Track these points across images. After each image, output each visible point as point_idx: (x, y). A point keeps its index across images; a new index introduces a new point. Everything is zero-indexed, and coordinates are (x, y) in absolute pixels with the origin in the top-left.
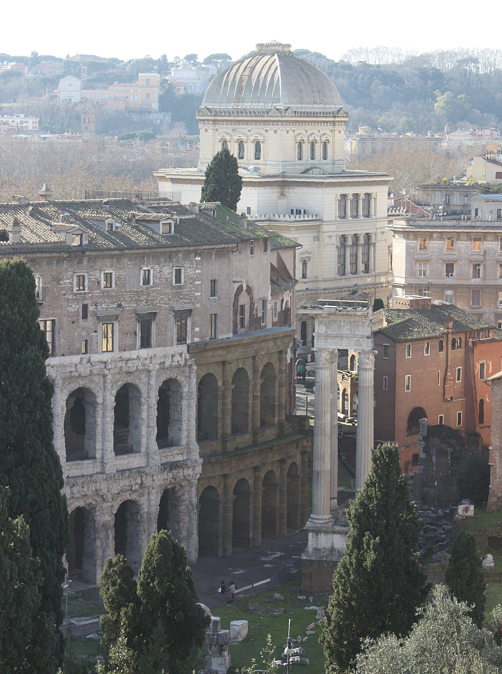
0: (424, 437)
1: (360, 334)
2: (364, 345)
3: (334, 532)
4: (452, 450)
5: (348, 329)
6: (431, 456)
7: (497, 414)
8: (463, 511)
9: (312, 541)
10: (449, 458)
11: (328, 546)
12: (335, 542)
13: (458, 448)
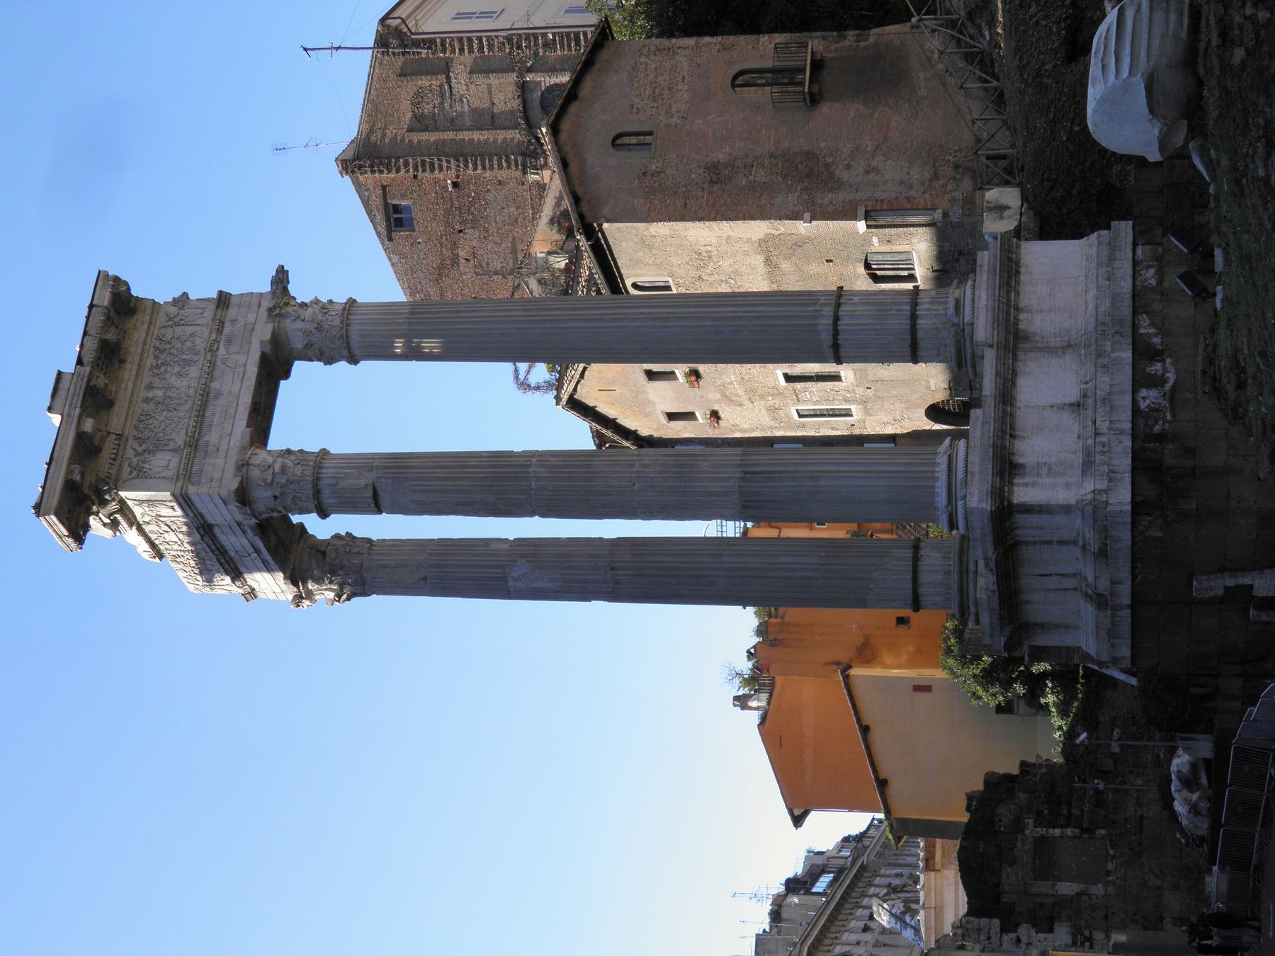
0: (1004, 929)
1: (207, 332)
2: (251, 318)
3: (1006, 396)
5: (179, 375)
6: (1062, 902)
8: (1001, 217)
9: (1053, 486)
10: (1057, 832)
12: (1052, 400)
13: (1022, 797)
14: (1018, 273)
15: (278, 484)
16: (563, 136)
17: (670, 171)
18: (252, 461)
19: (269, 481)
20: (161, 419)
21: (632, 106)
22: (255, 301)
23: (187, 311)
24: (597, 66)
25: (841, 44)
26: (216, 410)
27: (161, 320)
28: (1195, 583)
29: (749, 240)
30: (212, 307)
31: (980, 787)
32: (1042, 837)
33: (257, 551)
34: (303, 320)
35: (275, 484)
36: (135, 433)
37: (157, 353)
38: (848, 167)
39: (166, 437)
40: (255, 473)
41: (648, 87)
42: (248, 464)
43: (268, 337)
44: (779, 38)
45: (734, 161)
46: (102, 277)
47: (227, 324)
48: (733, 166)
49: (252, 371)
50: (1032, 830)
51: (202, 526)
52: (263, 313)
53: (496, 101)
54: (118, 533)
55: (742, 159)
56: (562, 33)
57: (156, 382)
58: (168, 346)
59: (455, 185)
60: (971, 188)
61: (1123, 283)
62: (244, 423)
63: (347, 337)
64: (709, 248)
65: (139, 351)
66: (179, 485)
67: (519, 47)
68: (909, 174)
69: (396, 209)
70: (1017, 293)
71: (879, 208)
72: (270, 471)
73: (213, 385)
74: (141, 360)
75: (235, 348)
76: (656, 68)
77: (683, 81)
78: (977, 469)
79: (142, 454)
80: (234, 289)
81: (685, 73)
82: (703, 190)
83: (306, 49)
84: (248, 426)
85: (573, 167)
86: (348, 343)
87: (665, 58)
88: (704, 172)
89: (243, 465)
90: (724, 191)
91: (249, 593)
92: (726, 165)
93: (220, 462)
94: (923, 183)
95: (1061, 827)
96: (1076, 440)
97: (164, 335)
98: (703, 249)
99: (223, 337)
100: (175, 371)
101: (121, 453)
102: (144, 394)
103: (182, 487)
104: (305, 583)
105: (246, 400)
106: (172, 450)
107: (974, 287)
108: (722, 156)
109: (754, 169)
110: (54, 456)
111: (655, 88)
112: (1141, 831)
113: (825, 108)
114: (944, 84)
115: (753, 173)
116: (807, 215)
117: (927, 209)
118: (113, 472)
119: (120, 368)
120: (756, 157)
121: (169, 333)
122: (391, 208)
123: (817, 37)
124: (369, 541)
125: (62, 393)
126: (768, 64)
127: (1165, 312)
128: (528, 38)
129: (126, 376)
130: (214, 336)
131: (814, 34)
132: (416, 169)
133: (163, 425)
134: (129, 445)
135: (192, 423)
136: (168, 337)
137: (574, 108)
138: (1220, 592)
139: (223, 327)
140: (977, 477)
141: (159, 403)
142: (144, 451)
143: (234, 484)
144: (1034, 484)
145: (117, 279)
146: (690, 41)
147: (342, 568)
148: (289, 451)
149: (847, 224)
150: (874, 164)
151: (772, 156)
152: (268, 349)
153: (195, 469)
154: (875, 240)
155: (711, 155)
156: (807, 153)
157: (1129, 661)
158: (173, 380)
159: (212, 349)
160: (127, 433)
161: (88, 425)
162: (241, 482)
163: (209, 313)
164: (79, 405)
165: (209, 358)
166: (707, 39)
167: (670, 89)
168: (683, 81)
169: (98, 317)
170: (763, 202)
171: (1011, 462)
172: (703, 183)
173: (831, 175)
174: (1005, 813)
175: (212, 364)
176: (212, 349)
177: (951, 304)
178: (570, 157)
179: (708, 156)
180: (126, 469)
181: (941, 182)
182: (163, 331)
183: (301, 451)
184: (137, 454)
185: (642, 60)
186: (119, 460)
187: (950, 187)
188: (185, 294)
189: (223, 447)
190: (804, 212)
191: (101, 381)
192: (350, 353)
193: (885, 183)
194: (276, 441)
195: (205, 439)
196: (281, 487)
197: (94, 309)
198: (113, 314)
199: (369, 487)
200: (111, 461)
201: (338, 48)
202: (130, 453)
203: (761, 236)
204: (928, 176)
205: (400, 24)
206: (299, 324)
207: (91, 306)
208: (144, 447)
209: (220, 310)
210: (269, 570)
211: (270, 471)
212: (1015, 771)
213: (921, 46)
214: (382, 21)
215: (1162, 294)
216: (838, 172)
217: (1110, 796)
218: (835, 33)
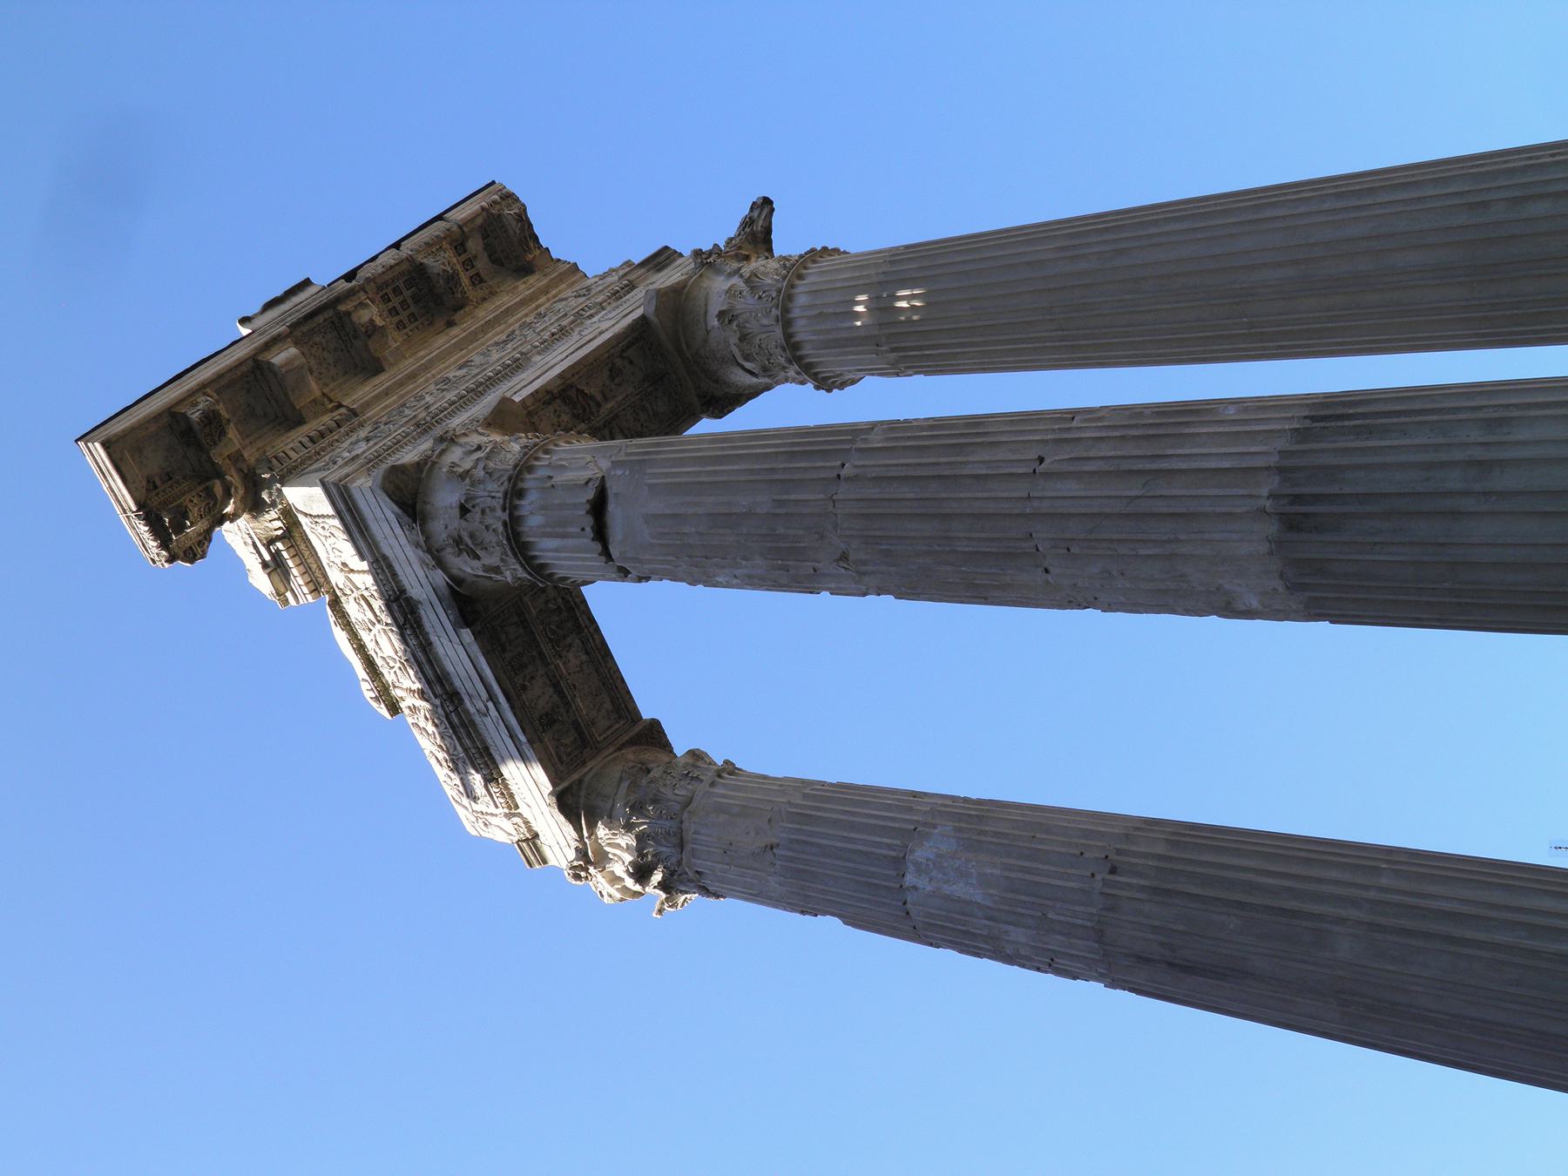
33: (492, 697)
51: (397, 599)
86: (786, 310)
91: (527, 840)
103: (347, 475)
104: (592, 827)
145: (509, 197)
147: (655, 801)
192: (788, 336)
199: (591, 484)
200: (305, 440)
207: (439, 217)
210: (524, 759)
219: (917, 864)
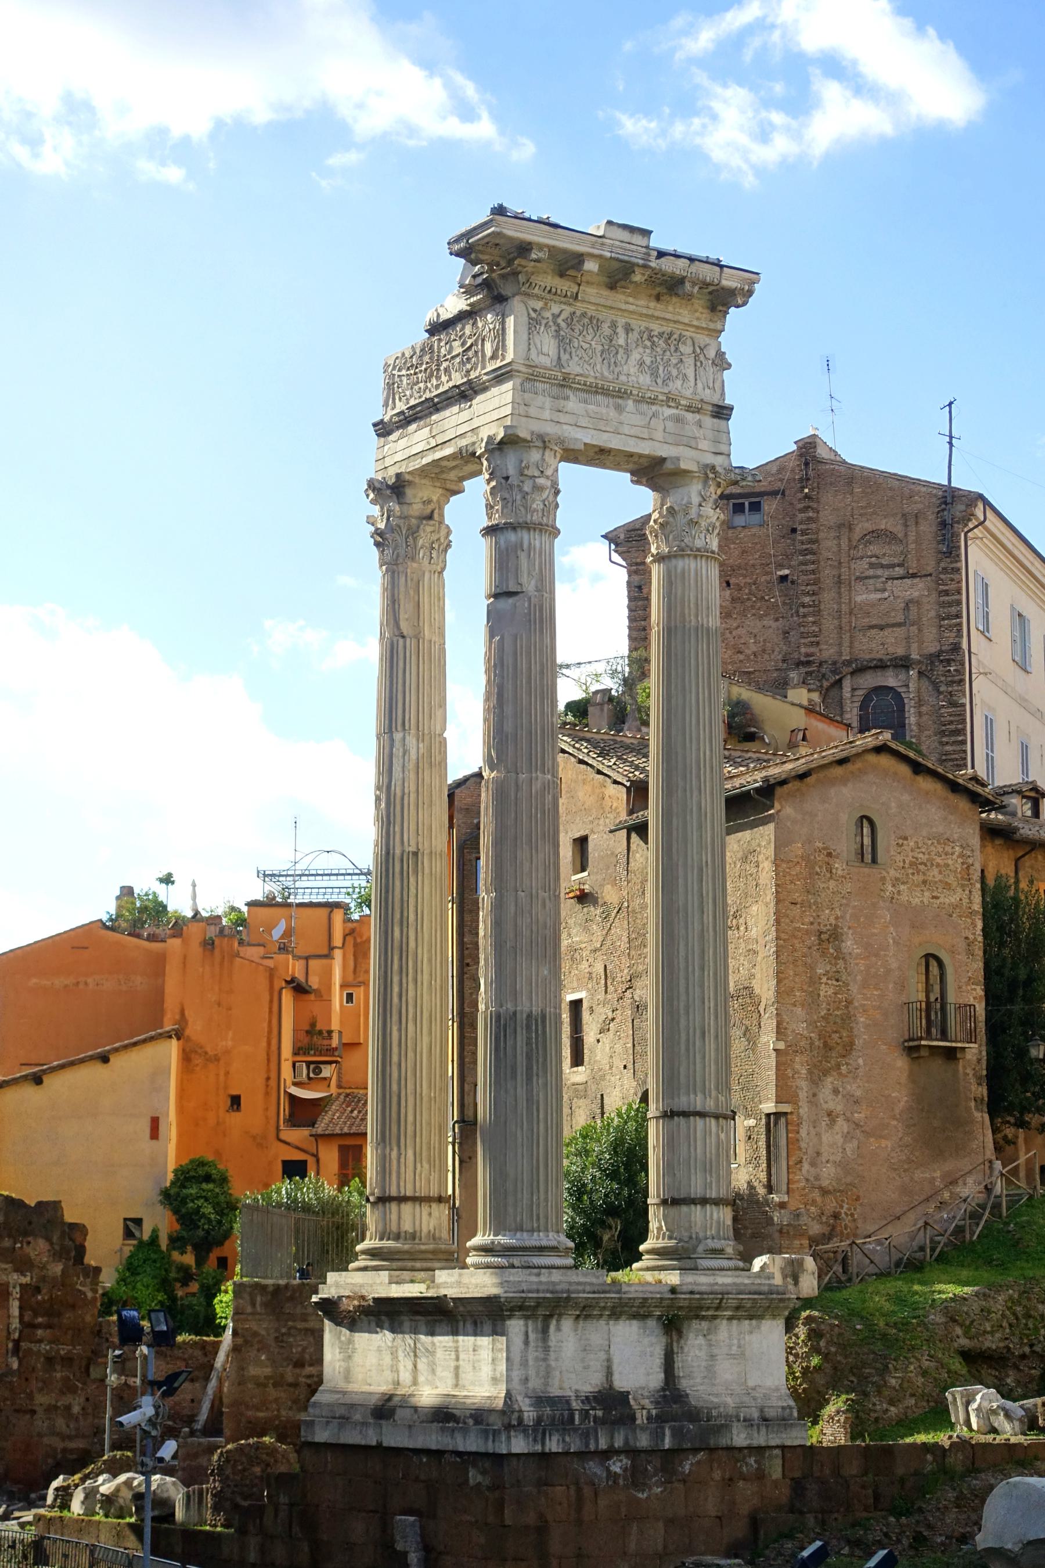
1: (688, 393)
4: (26, 1280)
5: (641, 363)
7: (797, 910)
10: (15, 1311)
11: (590, 1382)
12: (616, 1360)
13: (57, 1269)
14: (751, 1318)
15: (522, 482)
16: (872, 758)
17: (832, 884)
18: (547, 453)
19: (526, 472)
20: (593, 343)
21: (906, 839)
22: (723, 448)
23: (711, 370)
24: (951, 796)
25: (973, 1081)
26: (603, 406)
27: (702, 339)
28: (412, 1519)
29: (752, 976)
30: (715, 400)
31: (69, 1217)
32: (9, 1294)
34: (700, 505)
35: (521, 478)
36: (578, 313)
37: (665, 335)
38: (836, 1091)
39: (573, 350)
40: (535, 456)
41: (927, 856)
42: (545, 448)
43: (683, 466)
44: (980, 1009)
45: (843, 958)
46: (752, 277)
47: (697, 416)
48: (836, 958)
49: (645, 448)
50: (17, 1280)
51: (472, 388)
52: (710, 459)
53: (886, 632)
54: (462, 290)
55: (846, 968)
56: (964, 715)
57: (634, 336)
58: (673, 348)
59: (783, 579)
60: (811, 1233)
61: (743, 1436)
62: (588, 441)
63: (683, 556)
64: (742, 928)
65: (669, 316)
66: (523, 369)
67: (949, 662)
68: (827, 1162)
69: (756, 507)
70: (730, 1318)
71: (790, 1128)
72: (537, 473)
73: (630, 402)
74: (658, 318)
75: (670, 425)
76: (948, 865)
77: (934, 897)
78: (543, 1279)
79: (555, 323)
80: (734, 423)
81: (941, 900)
82: (812, 923)
83: (950, 404)
84: (585, 444)
85: (838, 771)
86: (675, 556)
87: (959, 876)
88: (831, 925)
89: (544, 442)
90: (810, 948)
92: (838, 949)
93: (547, 414)
94: (817, 1178)
95: (21, 1316)
96: (573, 1388)
97: (684, 343)
98: (742, 921)
99: (683, 413)
100: (645, 358)
101: (556, 298)
102: (621, 321)
103: (519, 372)
105: (614, 443)
106: (559, 358)
107: (737, 1269)
108: (849, 945)
109: (835, 983)
110: (560, 230)
111: (926, 865)
112: (17, 1411)
113: (901, 1063)
114: (927, 1200)
115: (829, 982)
116: (781, 1045)
117: (788, 1184)
118: (536, 291)
119: (650, 296)
120: (848, 985)
121: (686, 349)
122: (757, 500)
123: (980, 1052)
124: (443, 569)
125: (625, 236)
126: (951, 998)
127: (712, 1483)
128: (960, 672)
129: (642, 302)
130: (683, 402)
131: (984, 1048)
132: (804, 533)
133: (586, 346)
134: (563, 307)
135: (591, 380)
136: (682, 348)
137: (904, 770)
138: (399, 1547)
139: (693, 412)
140: (534, 1279)
141: (611, 341)
142: (558, 325)
143: (523, 434)
144: (526, 1342)
145: (750, 293)
146: (977, 906)
148: (557, 492)
149: (771, 1092)
150: (840, 1121)
151: (849, 1002)
152: (669, 466)
153: (540, 386)
154: (752, 1122)
155: (851, 932)
156: (852, 1044)
157: (310, 1439)
158: (635, 356)
159: (670, 400)
160: (578, 304)
161: (591, 266)
162: (525, 440)
163: (708, 395)
164: (613, 255)
165: (661, 397)
166: (980, 925)
167: (924, 882)
168: (934, 897)
169: (708, 273)
170: (798, 994)
171: (551, 1316)
172: (819, 924)
173: (826, 1073)
174: (38, 1249)
175: (652, 401)
176: (670, 400)
177: (717, 1244)
178: (849, 767)
179: (849, 928)
180: (538, 305)
181: (819, 1199)
182: (689, 342)
183: (557, 506)
184: (556, 317)
185: (957, 848)
186: (548, 296)
187: (813, 1209)
188: (729, 366)
189: (562, 418)
190: (786, 1042)
191: (638, 277)
193: (818, 1134)
194: (569, 474)
195: (571, 395)
196: (519, 486)
197: (717, 269)
198: (711, 288)
200: (548, 288)
201: (950, 443)
202: (555, 309)
203: (757, 991)
204: (825, 1183)
205: (977, 519)
206: (696, 500)
208: (563, 325)
209: (710, 408)
211: (537, 473)
212: (90, 1260)
213: (970, 1172)
214: (981, 497)
215: (731, 1479)
216: (830, 1079)
217: (59, 1375)
218: (985, 1073)
219: (404, 739)
